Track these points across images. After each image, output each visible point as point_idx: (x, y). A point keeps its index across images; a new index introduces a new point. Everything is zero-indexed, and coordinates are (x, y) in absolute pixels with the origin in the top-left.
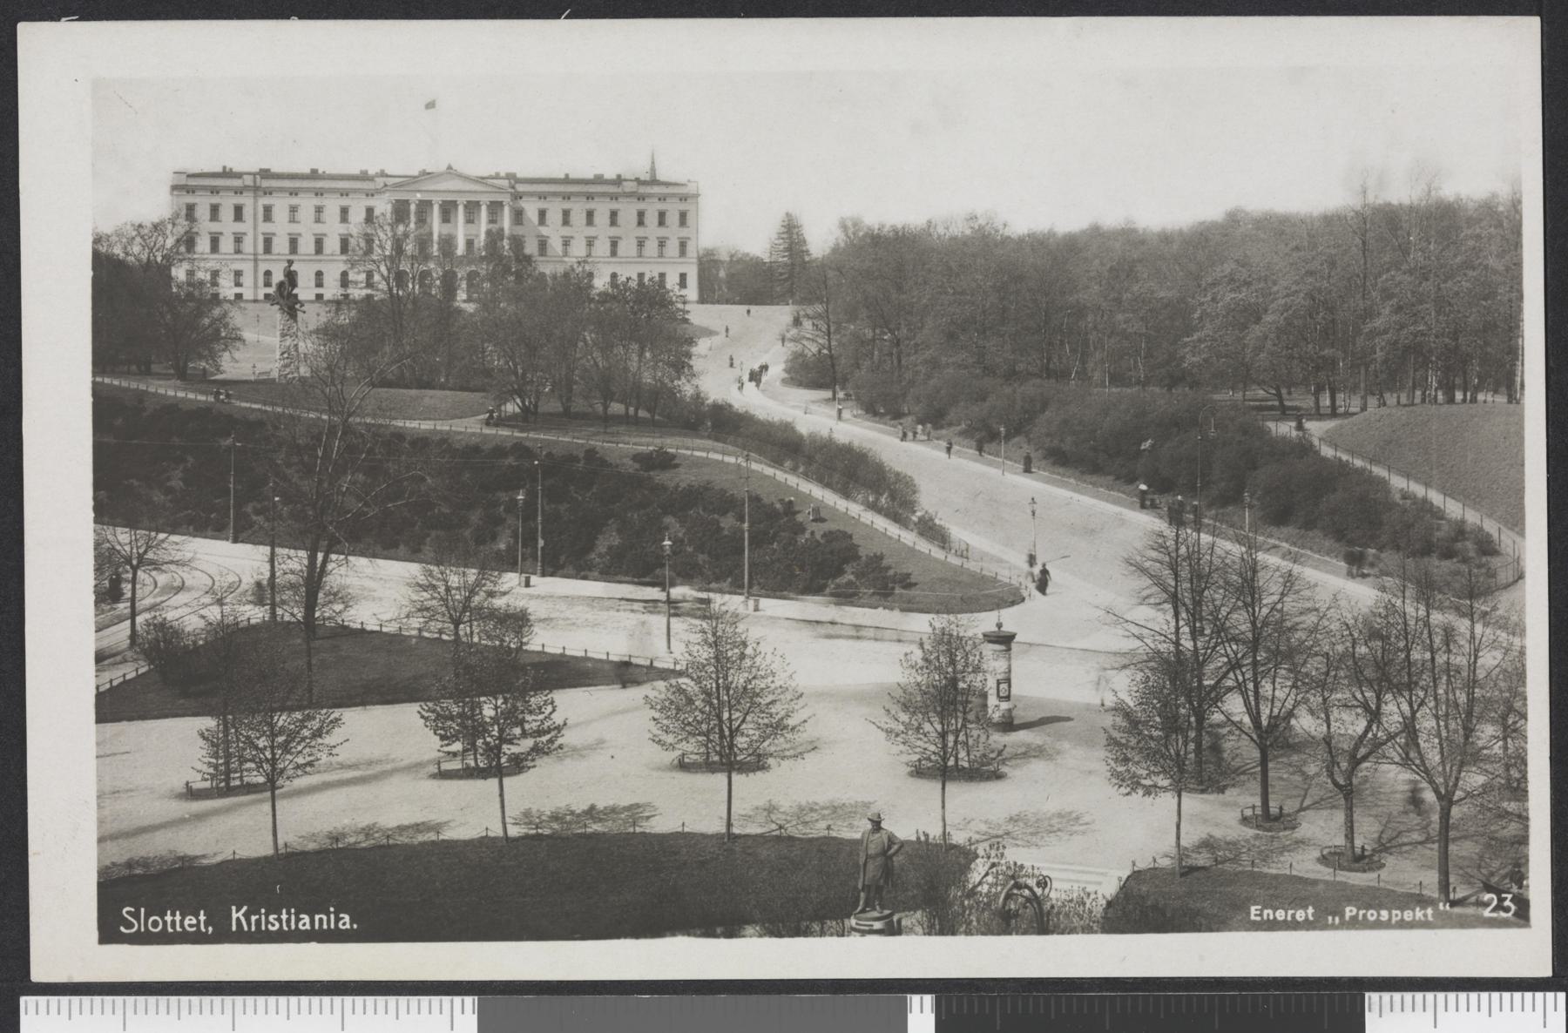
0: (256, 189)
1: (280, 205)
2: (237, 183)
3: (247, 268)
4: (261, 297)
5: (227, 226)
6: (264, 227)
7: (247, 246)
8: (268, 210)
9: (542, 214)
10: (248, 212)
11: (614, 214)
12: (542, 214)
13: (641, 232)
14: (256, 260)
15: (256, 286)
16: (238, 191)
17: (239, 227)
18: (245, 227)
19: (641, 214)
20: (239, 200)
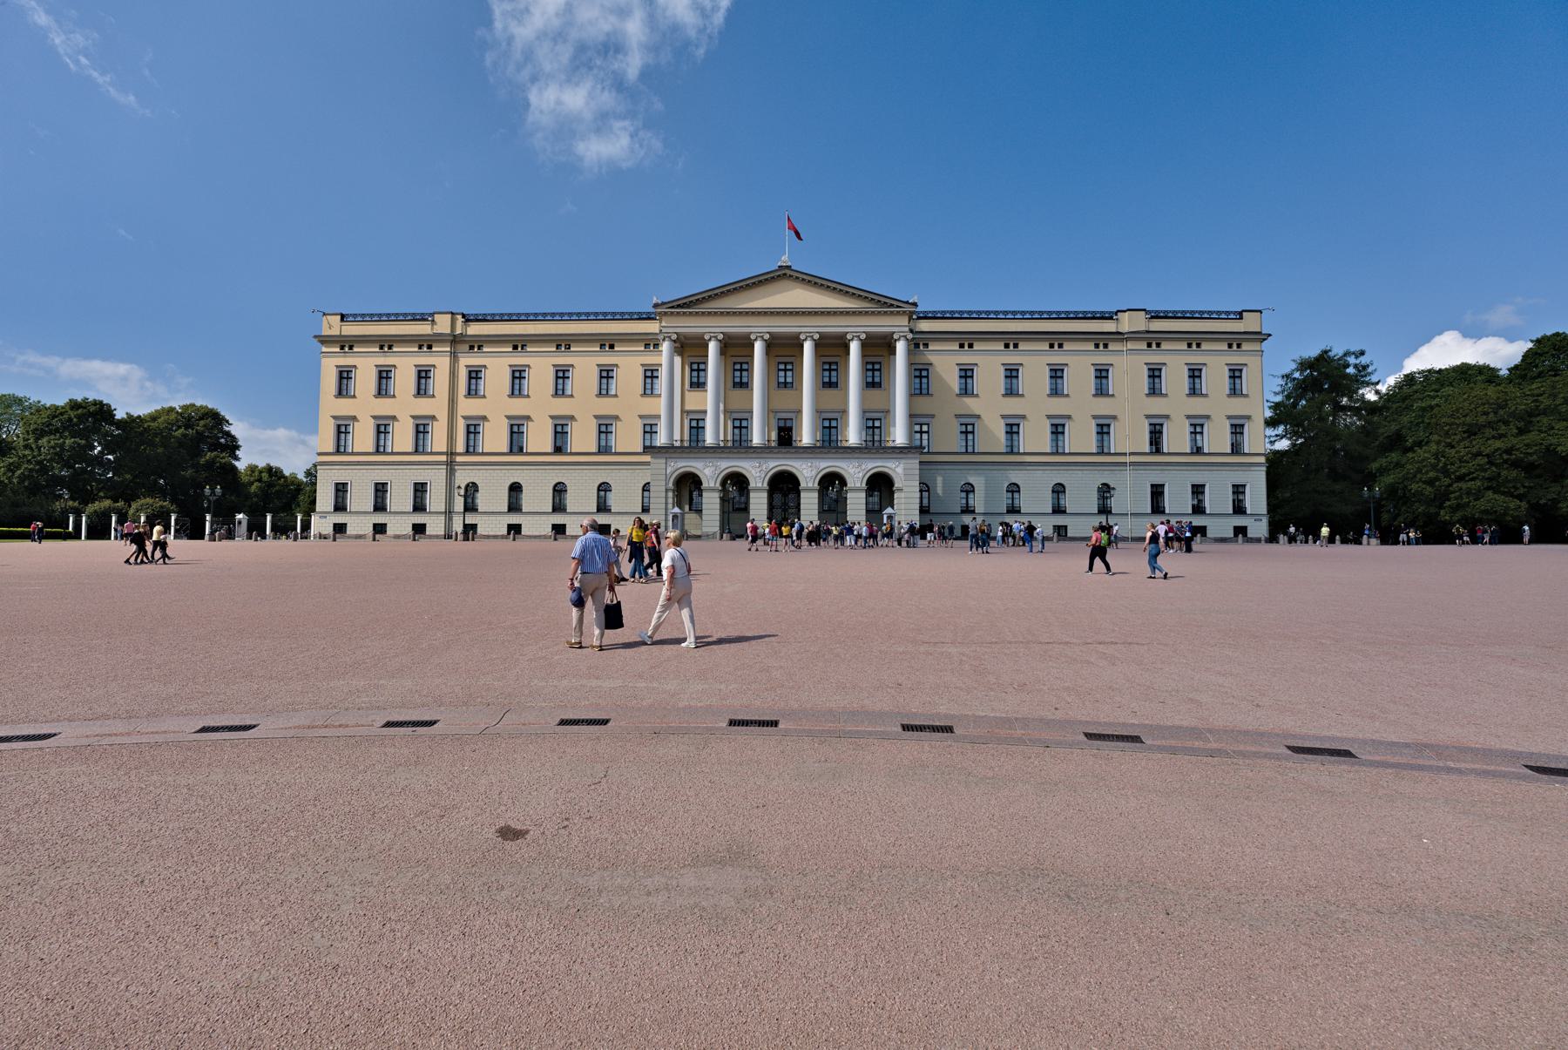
0: (454, 340)
1: (497, 367)
2: (423, 329)
3: (436, 479)
4: (458, 527)
5: (404, 405)
6: (467, 407)
7: (438, 440)
8: (474, 375)
9: (966, 374)
10: (440, 382)
11: (1102, 374)
12: (966, 374)
13: (1157, 406)
14: (451, 466)
15: (449, 513)
16: (426, 343)
17: (424, 407)
18: (436, 406)
19: (1155, 373)
20: (425, 360)
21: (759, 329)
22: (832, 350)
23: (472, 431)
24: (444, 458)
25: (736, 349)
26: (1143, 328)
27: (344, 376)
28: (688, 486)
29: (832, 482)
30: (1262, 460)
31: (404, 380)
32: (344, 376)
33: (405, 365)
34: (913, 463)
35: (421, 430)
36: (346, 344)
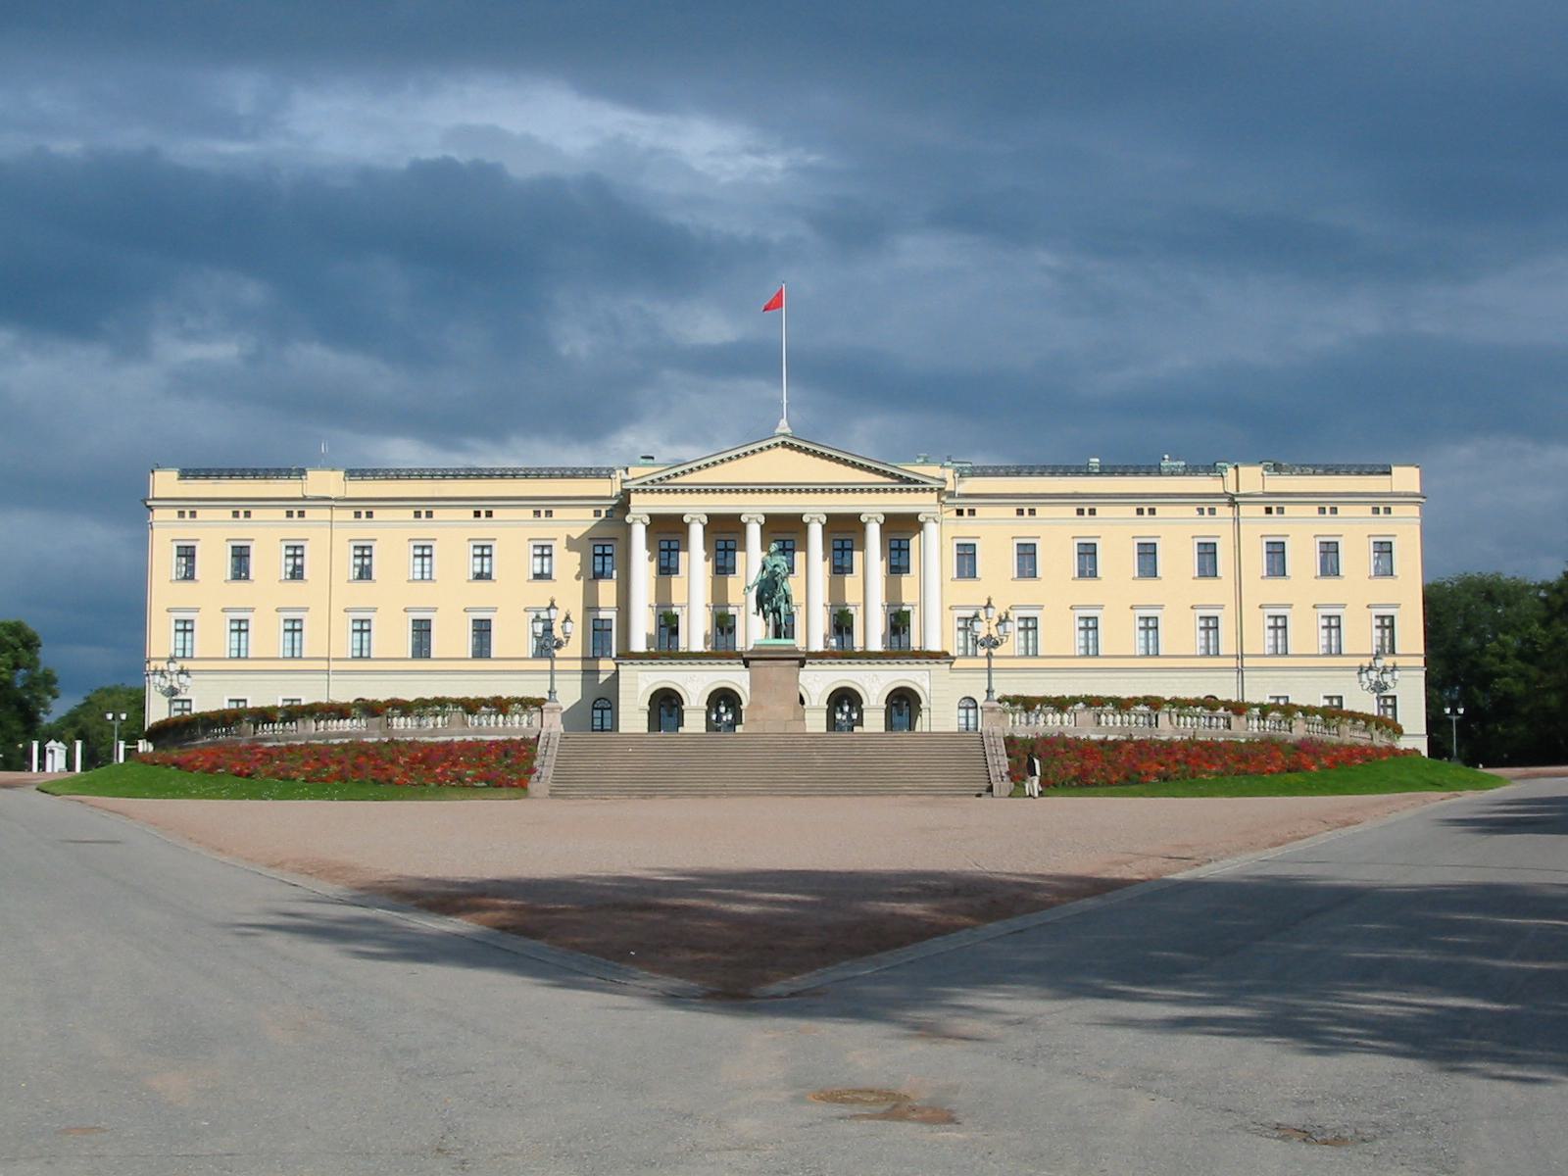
7: (313, 642)
16: (296, 508)
21: (753, 509)
22: (844, 533)
23: (363, 628)
24: (323, 665)
25: (725, 534)
26: (1259, 490)
27: (187, 553)
28: (666, 705)
29: (844, 699)
30: (1421, 662)
31: (268, 561)
32: (187, 553)
33: (267, 534)
34: (940, 669)
35: (294, 628)
36: (187, 508)
